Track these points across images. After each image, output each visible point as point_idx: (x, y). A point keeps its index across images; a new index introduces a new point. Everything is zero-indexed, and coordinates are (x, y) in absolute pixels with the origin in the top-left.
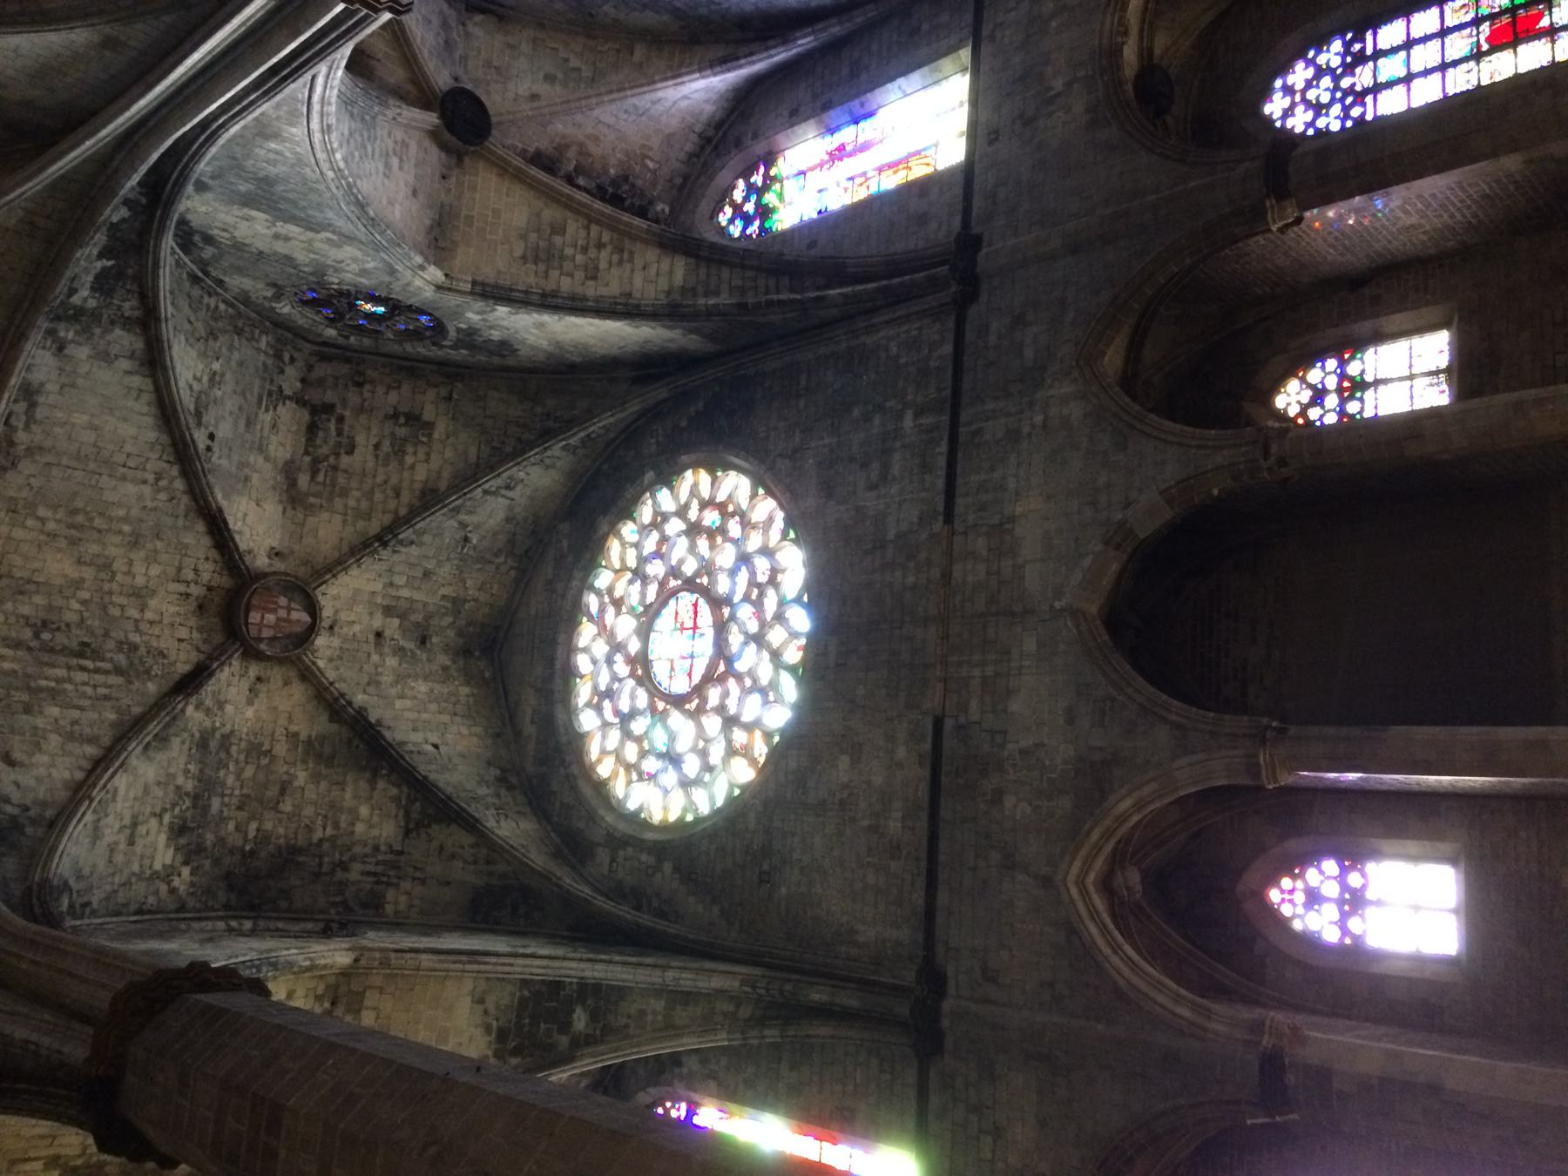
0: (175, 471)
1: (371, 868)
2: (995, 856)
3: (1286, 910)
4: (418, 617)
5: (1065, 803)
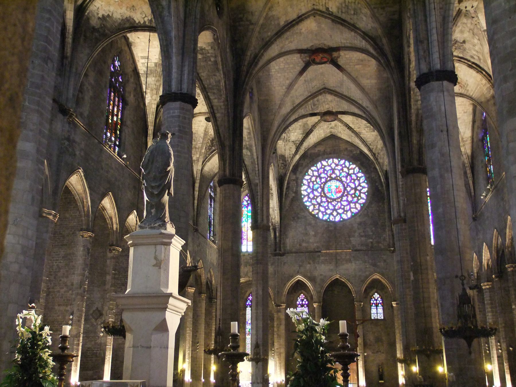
0: (351, 111)
1: (286, 137)
2: (301, 263)
3: (300, 296)
4: (335, 128)
5: (309, 274)
